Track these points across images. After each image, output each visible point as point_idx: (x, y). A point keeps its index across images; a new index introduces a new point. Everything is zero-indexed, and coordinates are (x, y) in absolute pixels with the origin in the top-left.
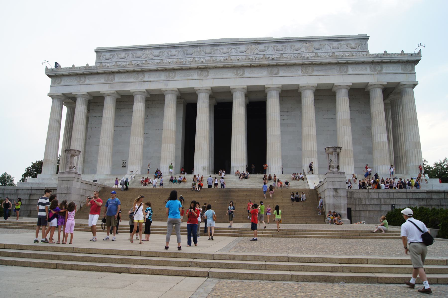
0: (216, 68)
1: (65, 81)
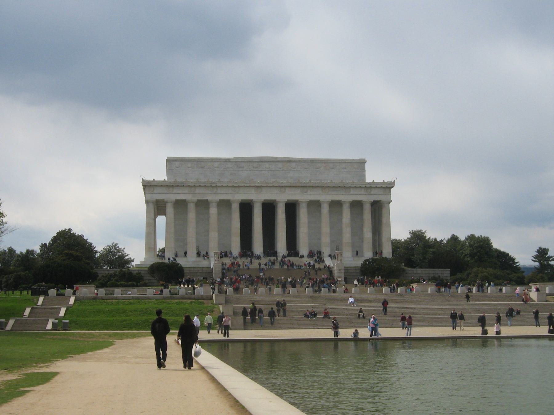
0: (267, 186)
1: (157, 190)
